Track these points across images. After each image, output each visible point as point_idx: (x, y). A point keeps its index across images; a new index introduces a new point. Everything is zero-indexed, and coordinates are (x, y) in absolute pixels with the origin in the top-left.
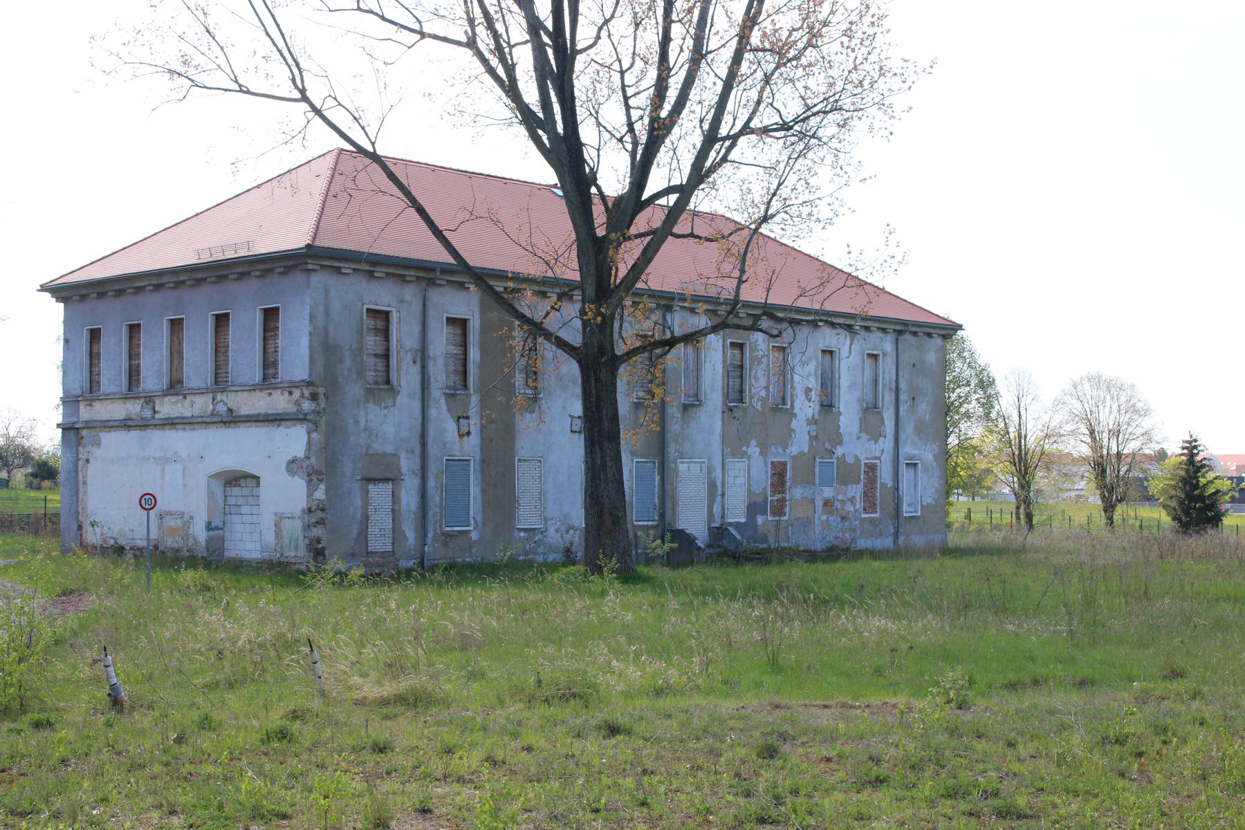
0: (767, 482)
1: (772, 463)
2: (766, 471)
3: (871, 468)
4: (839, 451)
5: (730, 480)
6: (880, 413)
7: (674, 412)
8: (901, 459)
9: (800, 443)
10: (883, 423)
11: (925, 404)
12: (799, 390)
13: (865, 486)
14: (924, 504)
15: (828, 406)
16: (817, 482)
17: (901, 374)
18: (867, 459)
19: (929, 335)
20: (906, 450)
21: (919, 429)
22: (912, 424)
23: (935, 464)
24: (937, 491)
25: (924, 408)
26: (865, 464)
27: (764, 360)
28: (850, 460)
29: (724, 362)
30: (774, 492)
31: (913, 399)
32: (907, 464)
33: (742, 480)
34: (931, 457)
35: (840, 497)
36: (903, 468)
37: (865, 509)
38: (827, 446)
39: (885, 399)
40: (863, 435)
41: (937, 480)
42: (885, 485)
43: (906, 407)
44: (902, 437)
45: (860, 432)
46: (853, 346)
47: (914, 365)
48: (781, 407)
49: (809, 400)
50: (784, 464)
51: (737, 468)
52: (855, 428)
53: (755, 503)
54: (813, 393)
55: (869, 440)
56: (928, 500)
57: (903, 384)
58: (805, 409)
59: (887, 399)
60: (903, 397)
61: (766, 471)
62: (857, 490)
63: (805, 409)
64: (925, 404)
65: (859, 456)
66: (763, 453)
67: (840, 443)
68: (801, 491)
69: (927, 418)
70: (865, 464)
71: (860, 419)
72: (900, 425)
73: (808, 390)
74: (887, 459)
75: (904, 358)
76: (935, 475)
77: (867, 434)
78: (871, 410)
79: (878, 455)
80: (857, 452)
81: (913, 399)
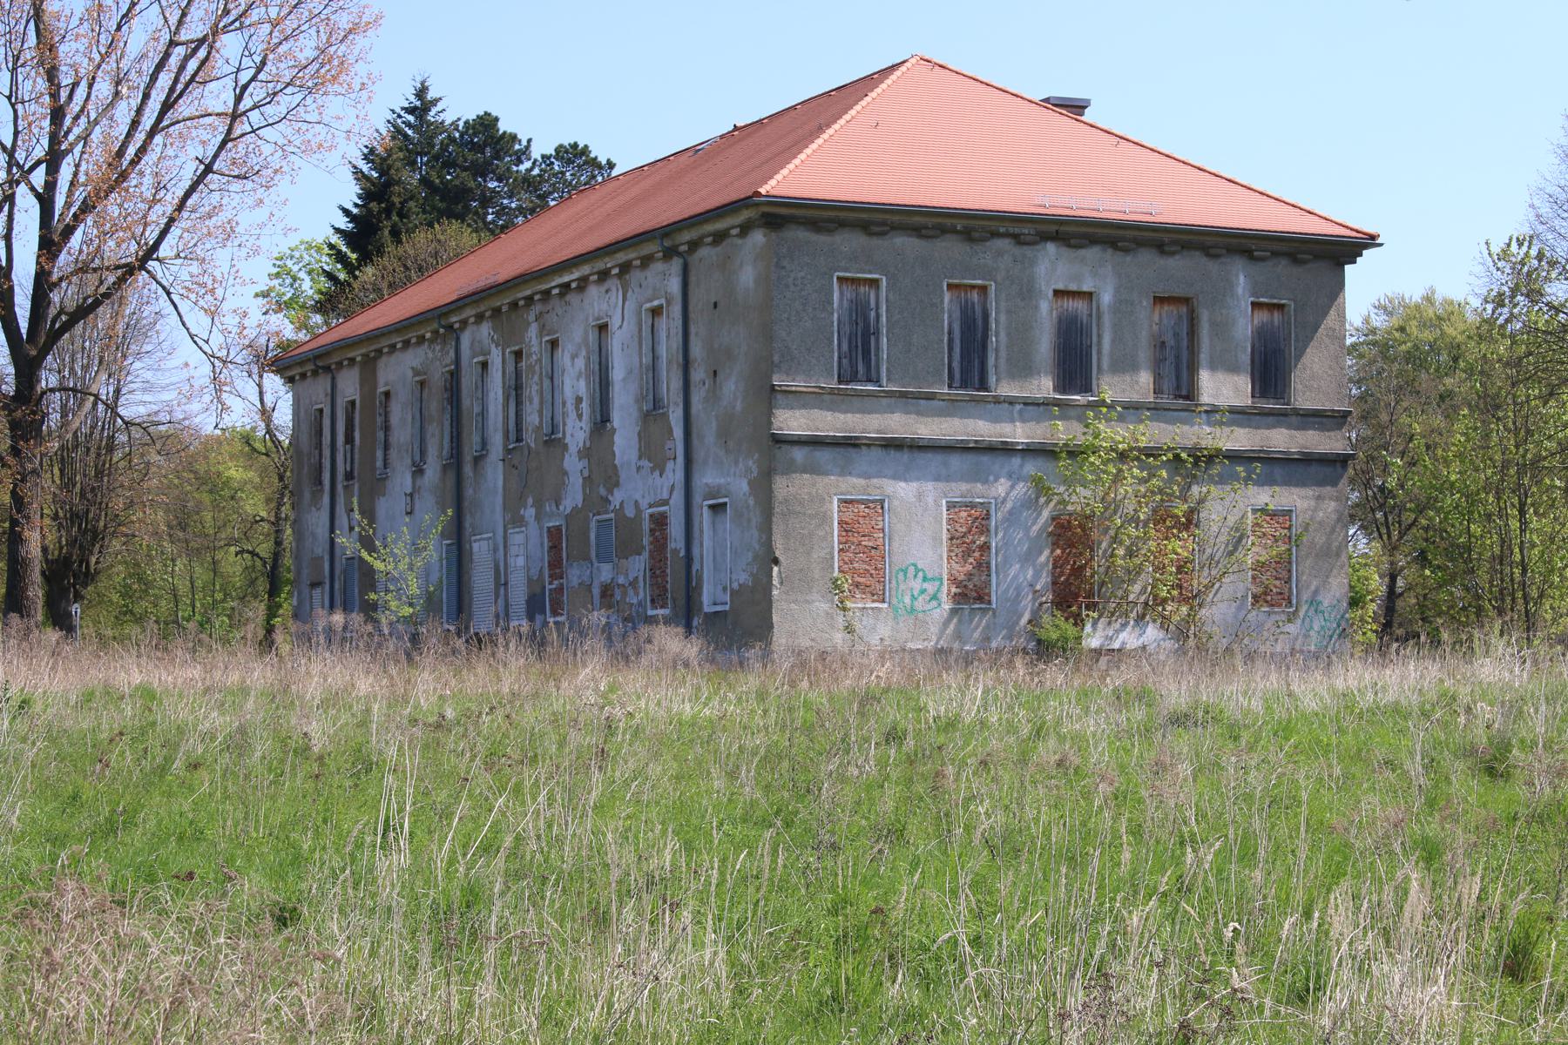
0: (542, 560)
1: (549, 528)
2: (542, 544)
3: (660, 521)
4: (617, 498)
5: (511, 561)
6: (665, 416)
7: (468, 469)
8: (697, 498)
9: (574, 497)
10: (670, 431)
11: (733, 379)
12: (570, 407)
13: (651, 556)
14: (735, 586)
15: (602, 422)
16: (593, 554)
17: (693, 329)
18: (651, 506)
19: (720, 237)
20: (707, 478)
21: (724, 434)
22: (714, 424)
23: (751, 502)
24: (755, 558)
25: (732, 388)
26: (651, 516)
27: (537, 368)
28: (630, 512)
29: (504, 383)
30: (553, 577)
31: (715, 372)
32: (712, 507)
33: (521, 561)
34: (744, 486)
35: (621, 580)
36: (704, 517)
37: (653, 601)
38: (603, 491)
39: (672, 388)
40: (646, 463)
41: (756, 533)
42: (675, 551)
43: (703, 393)
44: (699, 454)
45: (640, 458)
46: (627, 303)
47: (715, 305)
48: (553, 441)
49: (580, 420)
50: (558, 528)
51: (517, 538)
52: (633, 454)
53: (535, 595)
54: (584, 405)
55: (652, 470)
56: (743, 578)
57: (696, 350)
58: (576, 432)
59: (671, 385)
60: (698, 374)
61: (542, 544)
62: (638, 565)
63: (576, 432)
64: (733, 379)
65: (640, 501)
66: (538, 517)
67: (617, 484)
68: (578, 573)
69: (739, 406)
70: (651, 516)
71: (639, 434)
72: (694, 431)
73: (579, 400)
74: (678, 499)
75: (699, 298)
76: (754, 523)
77: (650, 461)
78: (652, 411)
79: (665, 495)
80: (638, 496)
81: (715, 372)
